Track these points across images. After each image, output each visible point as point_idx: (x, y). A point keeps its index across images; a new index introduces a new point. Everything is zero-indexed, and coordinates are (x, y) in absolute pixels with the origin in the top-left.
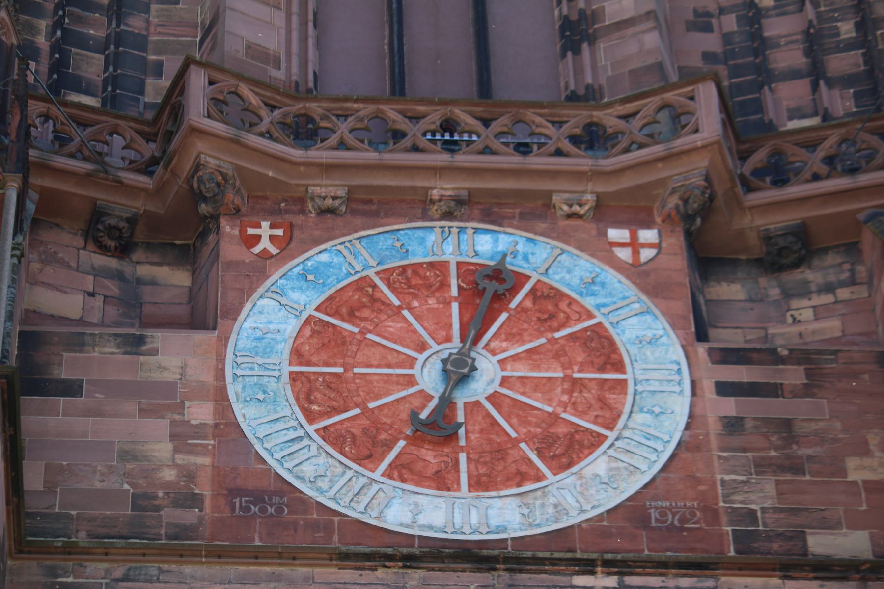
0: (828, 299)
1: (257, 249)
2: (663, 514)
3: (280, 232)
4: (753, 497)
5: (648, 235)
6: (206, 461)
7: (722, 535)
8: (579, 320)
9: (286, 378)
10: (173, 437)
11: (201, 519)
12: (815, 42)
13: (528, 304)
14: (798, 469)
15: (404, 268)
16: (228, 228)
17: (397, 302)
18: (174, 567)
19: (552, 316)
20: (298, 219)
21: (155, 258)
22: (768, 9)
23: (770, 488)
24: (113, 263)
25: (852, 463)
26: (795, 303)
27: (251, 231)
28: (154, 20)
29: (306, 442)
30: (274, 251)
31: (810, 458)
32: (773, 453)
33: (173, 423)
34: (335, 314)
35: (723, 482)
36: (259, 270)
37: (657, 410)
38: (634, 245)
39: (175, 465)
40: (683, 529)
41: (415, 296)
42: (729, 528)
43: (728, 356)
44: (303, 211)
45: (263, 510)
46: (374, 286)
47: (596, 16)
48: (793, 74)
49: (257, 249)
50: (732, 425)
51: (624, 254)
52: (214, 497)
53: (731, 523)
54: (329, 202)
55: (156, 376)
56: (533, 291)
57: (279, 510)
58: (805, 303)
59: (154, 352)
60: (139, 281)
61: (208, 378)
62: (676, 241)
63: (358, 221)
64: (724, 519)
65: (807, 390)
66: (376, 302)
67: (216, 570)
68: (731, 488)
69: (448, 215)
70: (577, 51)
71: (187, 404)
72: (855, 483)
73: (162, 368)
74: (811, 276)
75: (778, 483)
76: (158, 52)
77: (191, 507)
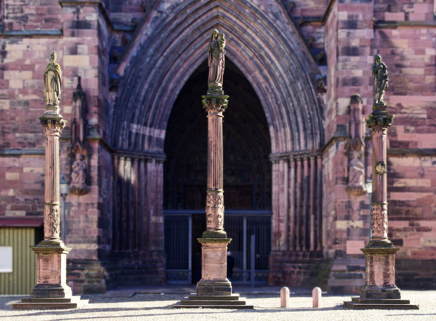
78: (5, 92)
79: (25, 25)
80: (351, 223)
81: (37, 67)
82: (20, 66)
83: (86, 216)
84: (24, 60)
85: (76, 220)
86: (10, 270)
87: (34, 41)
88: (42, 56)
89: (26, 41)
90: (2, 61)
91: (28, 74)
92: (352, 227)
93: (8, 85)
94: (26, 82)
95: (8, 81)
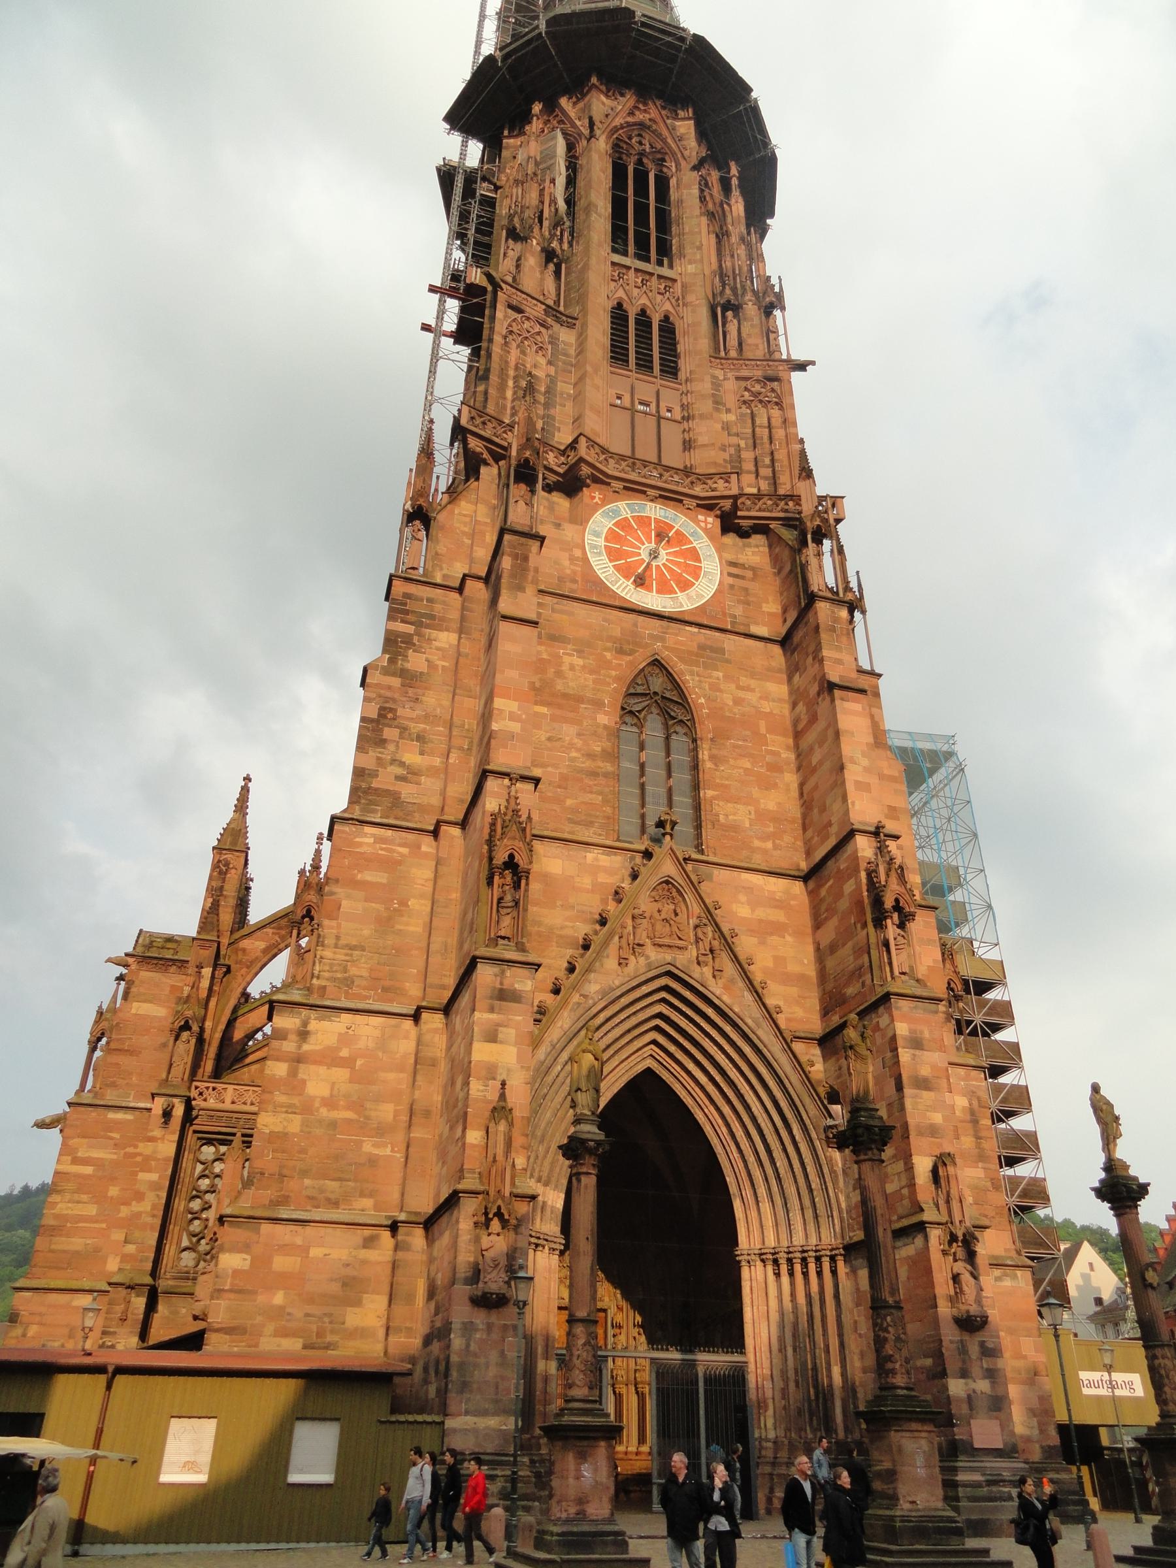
5: (710, 520)
6: (579, 569)
14: (748, 604)
24: (546, 494)
25: (764, 605)
36: (596, 508)
38: (705, 522)
43: (732, 564)
48: (749, 472)
50: (732, 587)
51: (703, 524)
61: (580, 541)
65: (753, 580)
69: (652, 501)
78: (296, 1101)
79: (347, 993)
80: (973, 1385)
81: (359, 1062)
82: (329, 1058)
83: (502, 1354)
84: (338, 1049)
85: (482, 1360)
86: (327, 1478)
87: (359, 1018)
88: (371, 1045)
89: (346, 1017)
90: (300, 1047)
91: (341, 1074)
92: (974, 1391)
93: (303, 1089)
94: (336, 1087)
95: (304, 1082)
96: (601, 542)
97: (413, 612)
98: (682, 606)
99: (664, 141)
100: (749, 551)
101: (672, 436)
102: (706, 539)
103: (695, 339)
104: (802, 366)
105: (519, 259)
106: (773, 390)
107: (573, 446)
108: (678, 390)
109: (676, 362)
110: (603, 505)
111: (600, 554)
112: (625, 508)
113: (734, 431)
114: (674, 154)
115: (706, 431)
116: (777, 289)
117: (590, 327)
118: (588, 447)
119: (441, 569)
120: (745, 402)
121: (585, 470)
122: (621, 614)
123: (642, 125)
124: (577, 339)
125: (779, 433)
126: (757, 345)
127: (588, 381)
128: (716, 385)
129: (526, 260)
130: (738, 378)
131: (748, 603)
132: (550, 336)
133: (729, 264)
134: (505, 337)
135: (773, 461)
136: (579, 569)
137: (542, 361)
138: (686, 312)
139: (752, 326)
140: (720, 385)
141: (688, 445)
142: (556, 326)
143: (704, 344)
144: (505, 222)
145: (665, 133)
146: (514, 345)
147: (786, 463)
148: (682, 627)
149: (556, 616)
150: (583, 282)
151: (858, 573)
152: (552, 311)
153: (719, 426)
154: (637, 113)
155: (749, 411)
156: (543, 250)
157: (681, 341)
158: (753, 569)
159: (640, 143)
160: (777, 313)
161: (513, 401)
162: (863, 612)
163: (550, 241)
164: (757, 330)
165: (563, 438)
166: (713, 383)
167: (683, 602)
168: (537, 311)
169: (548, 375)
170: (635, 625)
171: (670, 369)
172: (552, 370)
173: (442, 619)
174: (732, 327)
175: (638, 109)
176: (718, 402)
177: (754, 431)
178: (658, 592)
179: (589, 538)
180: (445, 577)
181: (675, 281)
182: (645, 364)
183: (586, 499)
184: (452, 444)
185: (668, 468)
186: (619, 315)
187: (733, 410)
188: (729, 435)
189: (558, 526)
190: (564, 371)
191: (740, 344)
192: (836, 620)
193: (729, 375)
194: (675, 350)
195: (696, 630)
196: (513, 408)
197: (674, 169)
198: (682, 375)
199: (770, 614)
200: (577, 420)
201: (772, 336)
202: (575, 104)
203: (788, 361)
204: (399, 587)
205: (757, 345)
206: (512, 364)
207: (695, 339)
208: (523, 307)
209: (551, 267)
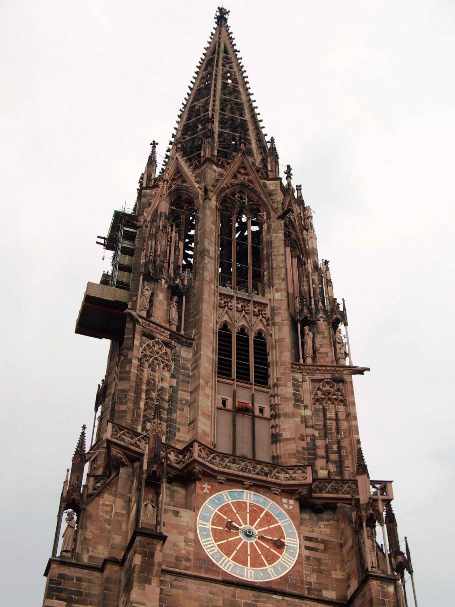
0: (327, 523)
1: (204, 491)
2: (292, 580)
3: (210, 487)
4: (311, 578)
5: (292, 502)
6: (192, 549)
7: (304, 588)
8: (276, 523)
9: (210, 529)
10: (185, 541)
11: (191, 565)
12: (327, 448)
13: (265, 517)
14: (321, 573)
15: (237, 502)
16: (198, 484)
17: (235, 511)
18: (185, 579)
19: (270, 521)
20: (214, 484)
21: (177, 485)
22: (317, 437)
23: (315, 576)
25: (333, 572)
26: (320, 522)
27: (203, 486)
28: (178, 415)
29: (214, 548)
30: (208, 492)
31: (324, 570)
32: (316, 567)
33: (185, 537)
34: (222, 513)
35: (305, 574)
36: (205, 497)
37: (292, 551)
38: (288, 504)
39: (185, 549)
40: (296, 585)
41: (240, 510)
42: (306, 586)
43: (308, 539)
44: (215, 482)
45: (204, 565)
46: (230, 506)
47: (281, 435)
48: (322, 457)
49: (204, 491)
50: (308, 558)
51: (286, 506)
52: (194, 559)
53: (306, 585)
54: (221, 481)
55: (181, 523)
56: (266, 513)
57: (208, 566)
58: (322, 523)
59: (181, 517)
60: (174, 491)
61: (193, 526)
62: (297, 505)
63: (227, 487)
64: (305, 583)
65: (324, 551)
66: (231, 510)
67: (194, 581)
68: (307, 575)
69: (247, 489)
70: (276, 443)
71: (188, 533)
72: (333, 578)
73: (183, 521)
74: (324, 516)
75: (317, 575)
76: (179, 425)
77: (189, 562)
96: (209, 526)
97: (66, 590)
98: (270, 577)
99: (259, 196)
100: (322, 524)
101: (263, 430)
102: (288, 518)
103: (281, 352)
104: (361, 371)
105: (152, 295)
106: (338, 390)
107: (189, 447)
108: (268, 393)
109: (267, 370)
110: (211, 494)
111: (208, 536)
112: (227, 496)
113: (310, 423)
114: (266, 205)
115: (288, 428)
116: (341, 309)
117: (203, 347)
118: (200, 450)
119: (88, 552)
120: (317, 400)
121: (198, 468)
122: (224, 587)
123: (242, 184)
124: (193, 356)
125: (344, 425)
126: (327, 353)
127: (201, 392)
128: (297, 386)
129: (157, 296)
130: (313, 380)
131: (320, 572)
132: (174, 355)
133: (306, 288)
134: (140, 360)
135: (339, 447)
136: (192, 549)
137: (167, 375)
138: (274, 330)
139: (323, 337)
140: (300, 386)
141: (275, 439)
142: (178, 347)
143: (287, 356)
144: (142, 270)
145: (259, 189)
146: (147, 365)
147: (349, 450)
148: (270, 595)
149: (174, 591)
150: (198, 311)
151: (406, 538)
152: (173, 335)
153: (299, 420)
154: (239, 176)
155: (321, 407)
156: (169, 287)
157: (270, 353)
158: (324, 542)
159: (241, 198)
160: (341, 326)
161: (145, 410)
162: (411, 572)
163: (175, 279)
164: (327, 341)
165: (183, 436)
166: (294, 385)
167: (271, 573)
168: (165, 336)
169: (171, 386)
170: (234, 596)
171: (262, 378)
172: (174, 382)
173: (88, 595)
174: (309, 340)
175: (240, 173)
176: (298, 400)
177: (325, 423)
178: (251, 566)
179: (199, 523)
180: (91, 558)
181: (266, 305)
182: (243, 376)
183: (198, 490)
184: (96, 410)
185: (260, 463)
186: (224, 334)
187: (309, 406)
188: (307, 427)
189: (176, 513)
190: (183, 381)
191: (314, 352)
192: (386, 594)
193: (307, 378)
194: (266, 360)
195: (280, 598)
196: (145, 416)
197: (265, 217)
198: (271, 382)
199: (337, 580)
200: (193, 422)
201: (338, 346)
202: (194, 170)
203: (350, 367)
204: (56, 570)
205: (327, 353)
206: (145, 380)
207: (281, 352)
208: (154, 334)
209: (175, 298)
